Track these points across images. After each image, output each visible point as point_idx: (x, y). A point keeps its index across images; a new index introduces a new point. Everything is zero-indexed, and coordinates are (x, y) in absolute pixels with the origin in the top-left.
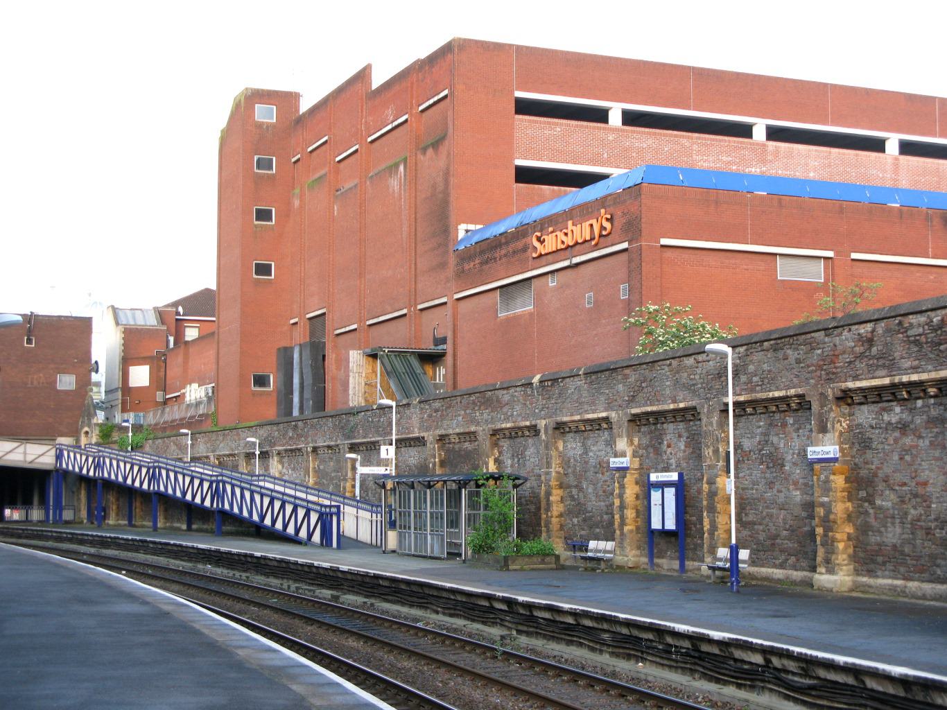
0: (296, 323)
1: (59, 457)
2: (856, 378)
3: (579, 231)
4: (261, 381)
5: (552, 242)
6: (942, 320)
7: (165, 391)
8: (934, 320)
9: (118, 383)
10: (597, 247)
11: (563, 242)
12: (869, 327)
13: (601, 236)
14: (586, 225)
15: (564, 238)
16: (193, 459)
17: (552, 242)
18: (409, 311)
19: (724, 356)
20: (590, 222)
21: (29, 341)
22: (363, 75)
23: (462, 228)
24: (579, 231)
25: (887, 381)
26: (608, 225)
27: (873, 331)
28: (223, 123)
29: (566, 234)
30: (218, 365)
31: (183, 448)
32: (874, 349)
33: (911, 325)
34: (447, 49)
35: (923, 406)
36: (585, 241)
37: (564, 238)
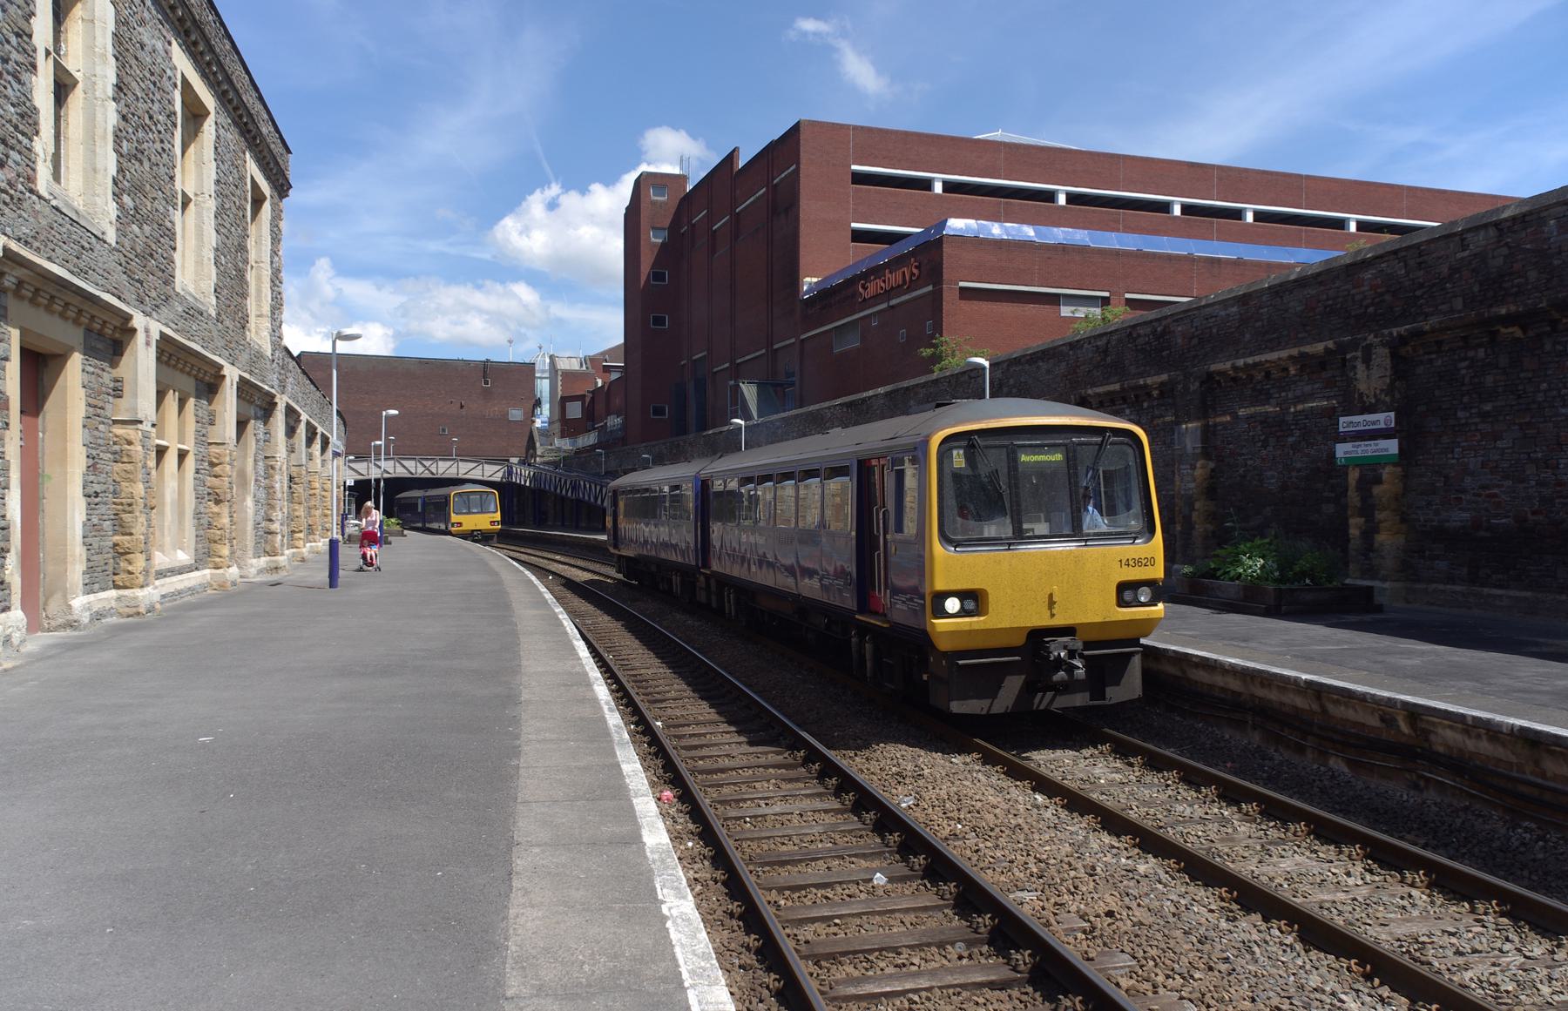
0: (684, 365)
1: (510, 473)
2: (1094, 385)
3: (894, 278)
4: (659, 411)
5: (874, 287)
6: (1164, 330)
7: (593, 421)
8: (1159, 329)
9: (556, 417)
10: (910, 290)
11: (882, 288)
12: (1104, 340)
13: (911, 278)
14: (899, 273)
15: (883, 285)
16: (606, 473)
17: (874, 287)
18: (767, 351)
19: (984, 368)
20: (901, 271)
21: (486, 383)
22: (730, 158)
23: (809, 281)
24: (894, 278)
25: (1117, 387)
26: (915, 271)
27: (1108, 342)
28: (627, 203)
29: (884, 281)
30: (53, 281)
31: (599, 464)
32: (1109, 359)
33: (1139, 335)
34: (796, 128)
35: (1149, 407)
36: (899, 286)
37: (883, 285)
